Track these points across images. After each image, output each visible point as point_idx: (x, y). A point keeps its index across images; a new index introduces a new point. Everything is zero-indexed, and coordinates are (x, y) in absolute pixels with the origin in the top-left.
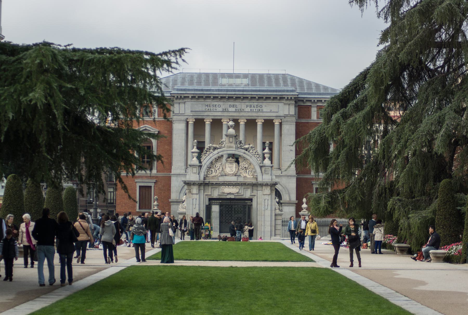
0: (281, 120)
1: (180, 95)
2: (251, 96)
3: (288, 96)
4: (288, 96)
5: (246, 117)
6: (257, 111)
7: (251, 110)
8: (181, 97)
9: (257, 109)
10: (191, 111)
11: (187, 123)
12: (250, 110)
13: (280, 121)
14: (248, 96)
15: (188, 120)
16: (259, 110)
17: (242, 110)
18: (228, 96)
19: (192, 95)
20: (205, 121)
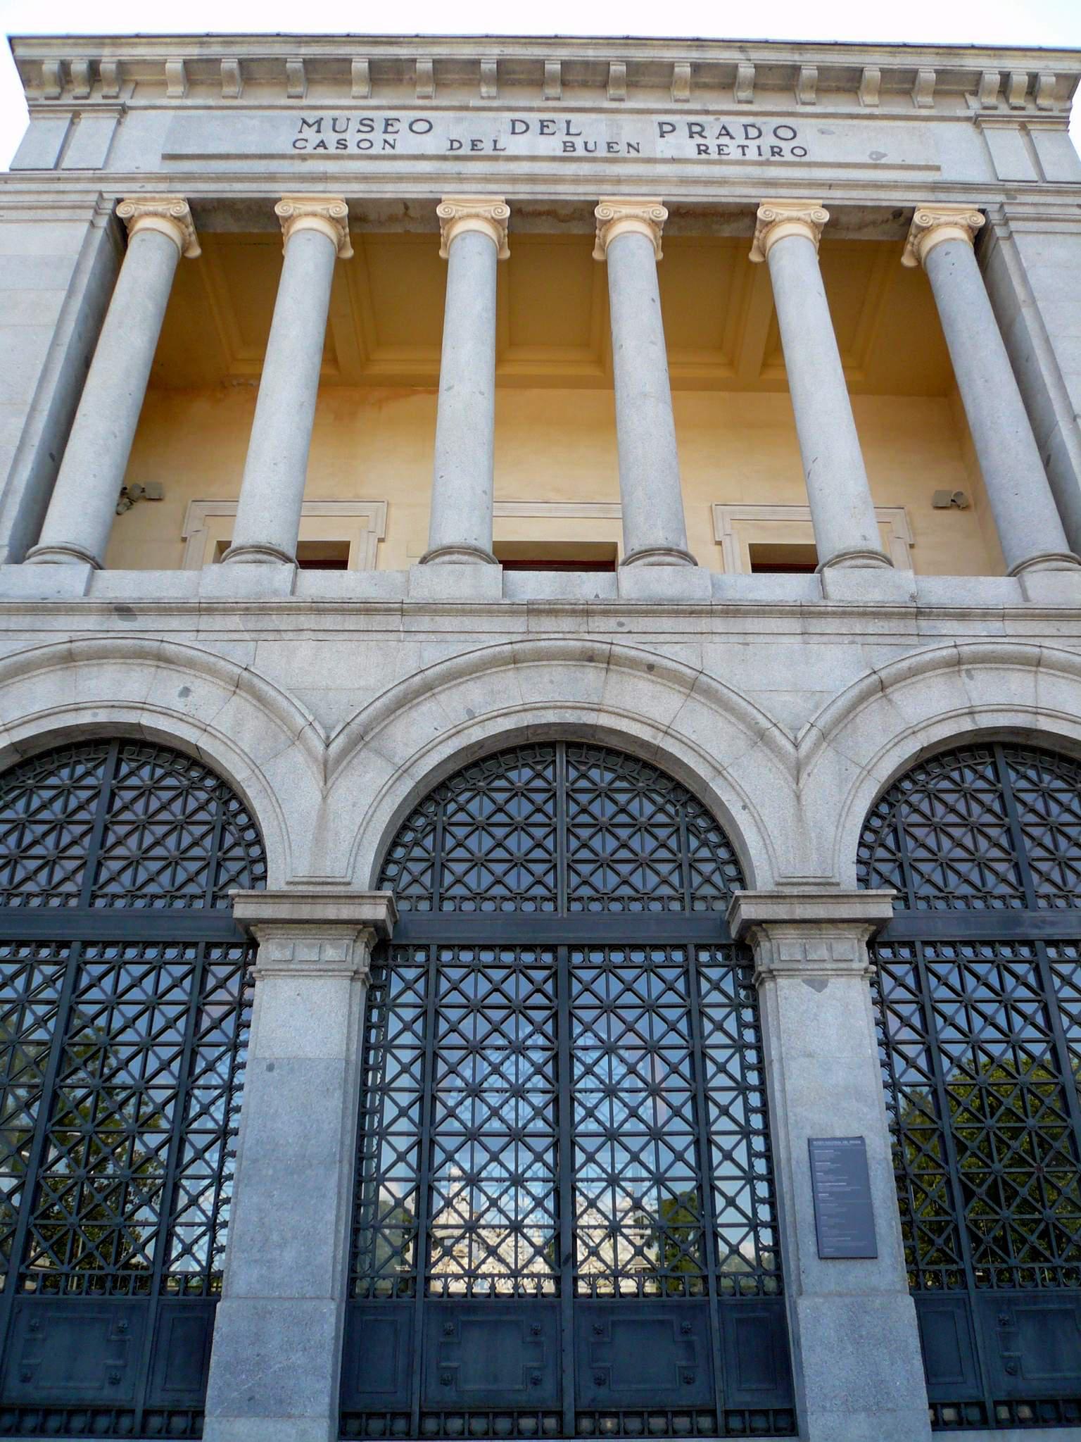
0: (983, 211)
1: (92, 52)
2: (695, 55)
3: (1009, 64)
4: (1009, 64)
5: (663, 189)
6: (752, 154)
7: (703, 150)
8: (94, 67)
9: (752, 145)
10: (169, 157)
11: (121, 232)
12: (691, 152)
13: (980, 220)
14: (668, 55)
15: (122, 212)
16: (776, 151)
17: (622, 148)
18: (495, 51)
19: (194, 51)
20: (279, 210)
